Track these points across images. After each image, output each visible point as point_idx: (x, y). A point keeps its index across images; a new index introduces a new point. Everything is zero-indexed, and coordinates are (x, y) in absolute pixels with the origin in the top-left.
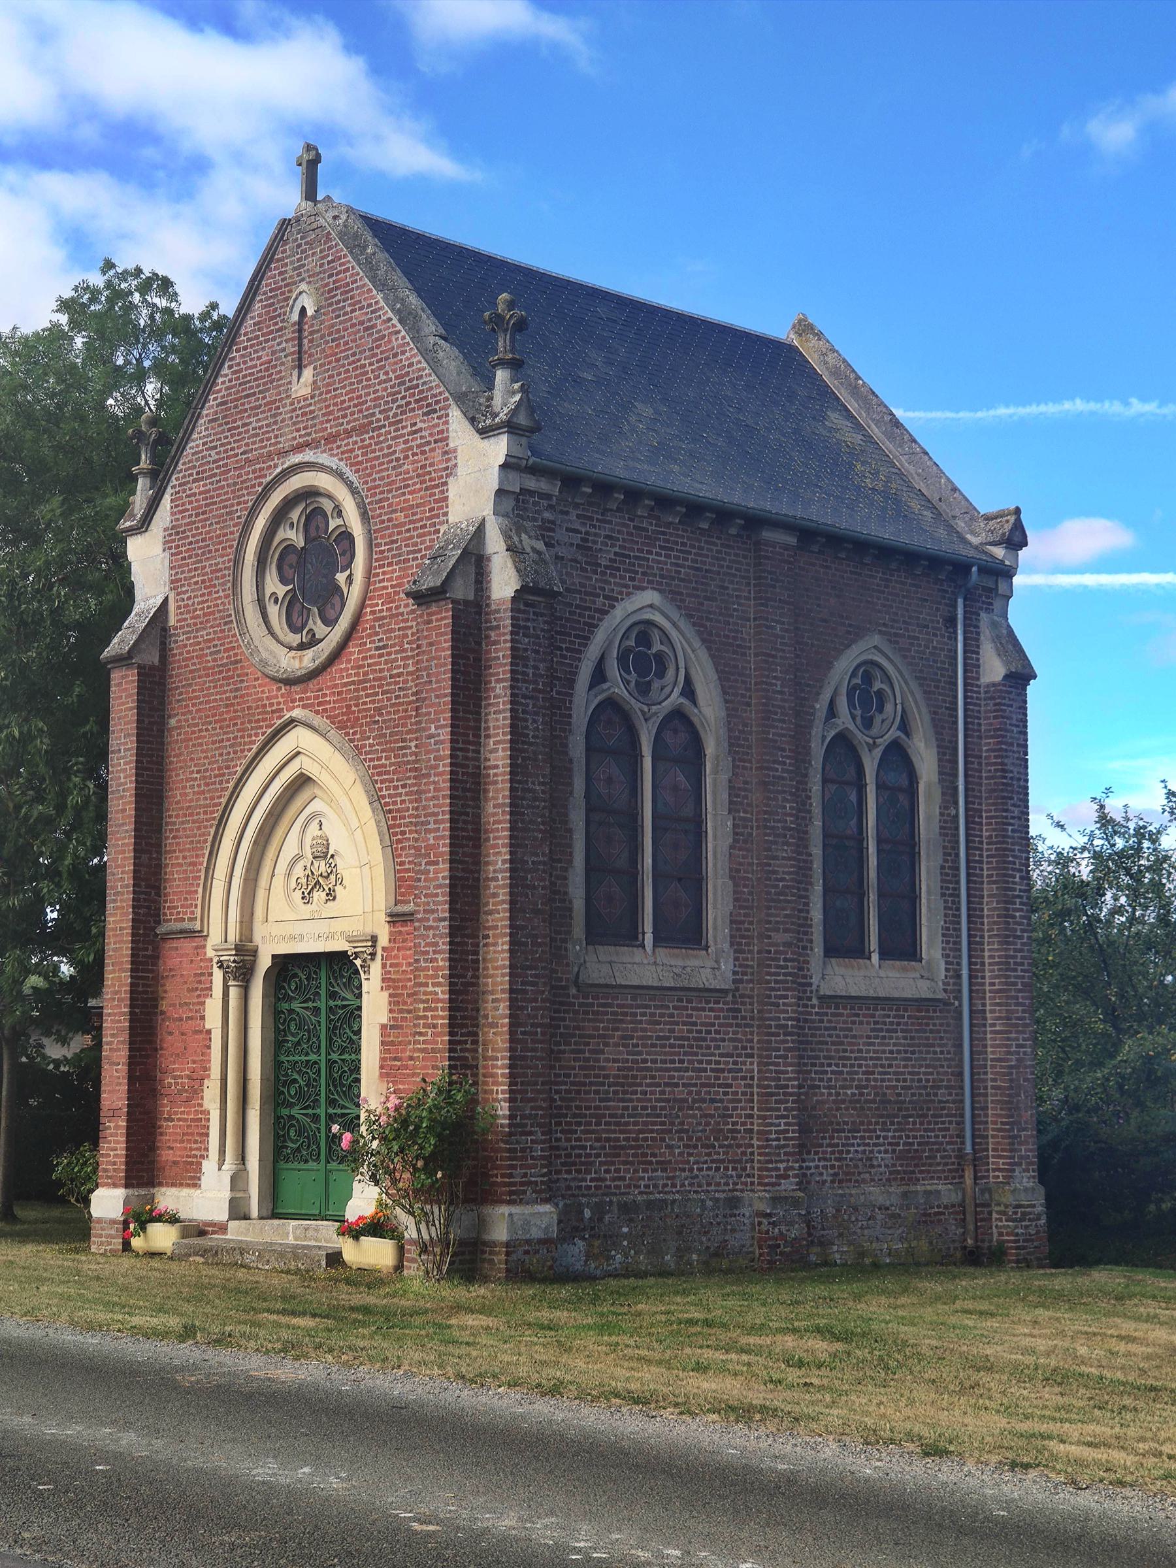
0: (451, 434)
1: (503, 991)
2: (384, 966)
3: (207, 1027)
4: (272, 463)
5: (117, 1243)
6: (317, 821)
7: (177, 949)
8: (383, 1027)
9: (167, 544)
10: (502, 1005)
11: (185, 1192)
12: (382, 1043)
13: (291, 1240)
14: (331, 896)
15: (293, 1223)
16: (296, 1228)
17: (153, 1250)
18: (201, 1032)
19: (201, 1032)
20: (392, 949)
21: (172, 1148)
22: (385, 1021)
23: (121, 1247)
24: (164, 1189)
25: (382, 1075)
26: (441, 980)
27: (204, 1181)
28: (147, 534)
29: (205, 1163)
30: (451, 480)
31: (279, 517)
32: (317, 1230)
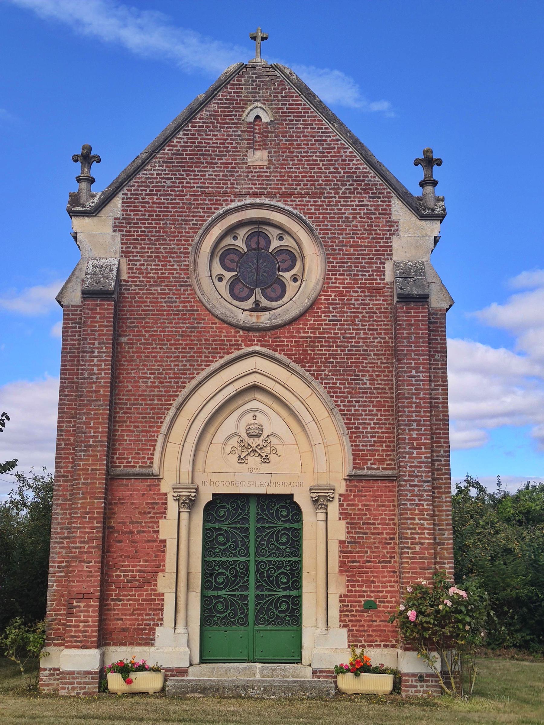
0: (393, 212)
1: (447, 524)
2: (341, 505)
3: (161, 537)
4: (229, 199)
5: (94, 687)
6: (252, 414)
7: (127, 485)
8: (341, 542)
9: (117, 228)
10: (447, 533)
11: (146, 648)
12: (341, 552)
13: (258, 677)
14: (266, 460)
15: (259, 665)
16: (263, 669)
17: (134, 691)
18: (155, 541)
19: (155, 541)
20: (349, 496)
21: (122, 620)
22: (343, 538)
23: (97, 690)
24: (113, 648)
25: (341, 572)
26: (426, 517)
27: (157, 642)
28: (95, 218)
29: (159, 630)
30: (394, 239)
31: (231, 231)
32: (284, 670)
